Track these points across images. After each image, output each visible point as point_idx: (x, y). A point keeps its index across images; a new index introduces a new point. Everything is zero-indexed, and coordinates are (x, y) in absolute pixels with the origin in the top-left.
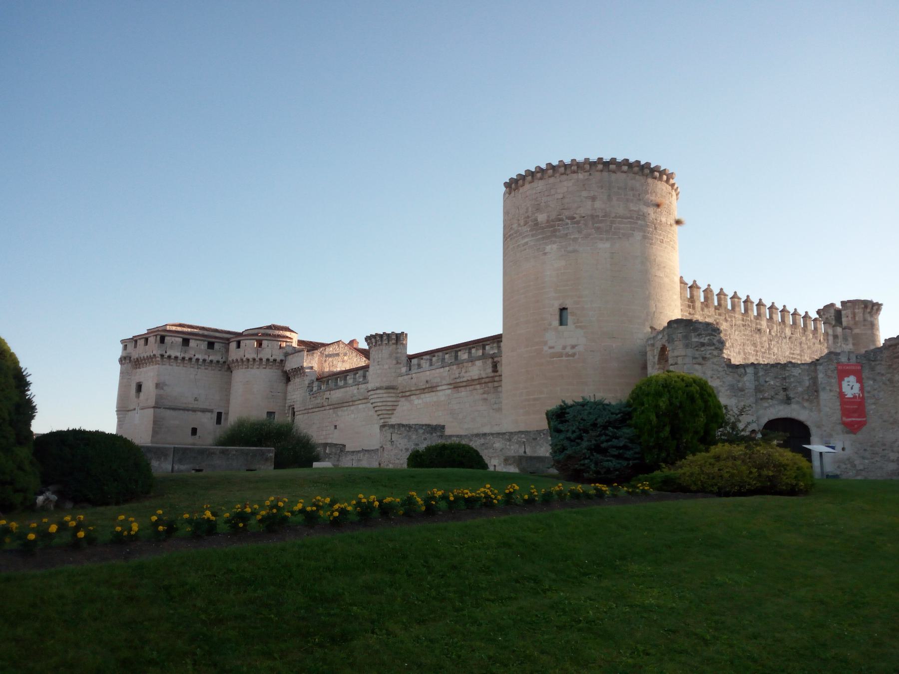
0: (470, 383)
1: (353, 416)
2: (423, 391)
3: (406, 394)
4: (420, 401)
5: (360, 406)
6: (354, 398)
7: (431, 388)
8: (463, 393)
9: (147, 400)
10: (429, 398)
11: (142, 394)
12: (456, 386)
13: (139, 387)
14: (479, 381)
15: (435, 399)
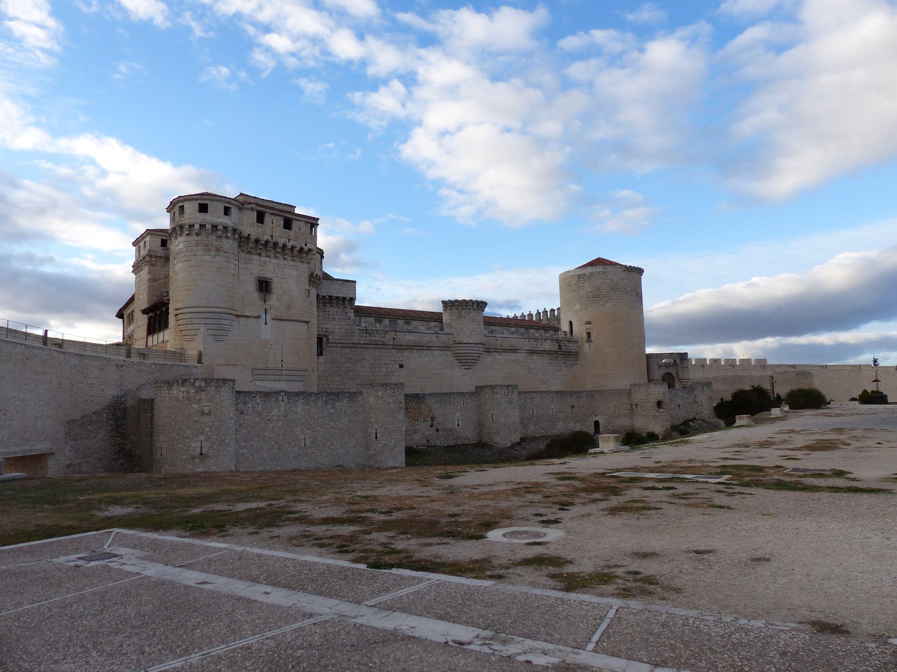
0: (544, 352)
1: (427, 359)
2: (506, 350)
3: (488, 350)
4: (501, 357)
5: (435, 352)
6: (432, 344)
7: (514, 350)
8: (535, 357)
9: (289, 308)
10: (508, 356)
11: (273, 300)
12: (532, 352)
13: (264, 286)
14: (548, 353)
15: (514, 357)
